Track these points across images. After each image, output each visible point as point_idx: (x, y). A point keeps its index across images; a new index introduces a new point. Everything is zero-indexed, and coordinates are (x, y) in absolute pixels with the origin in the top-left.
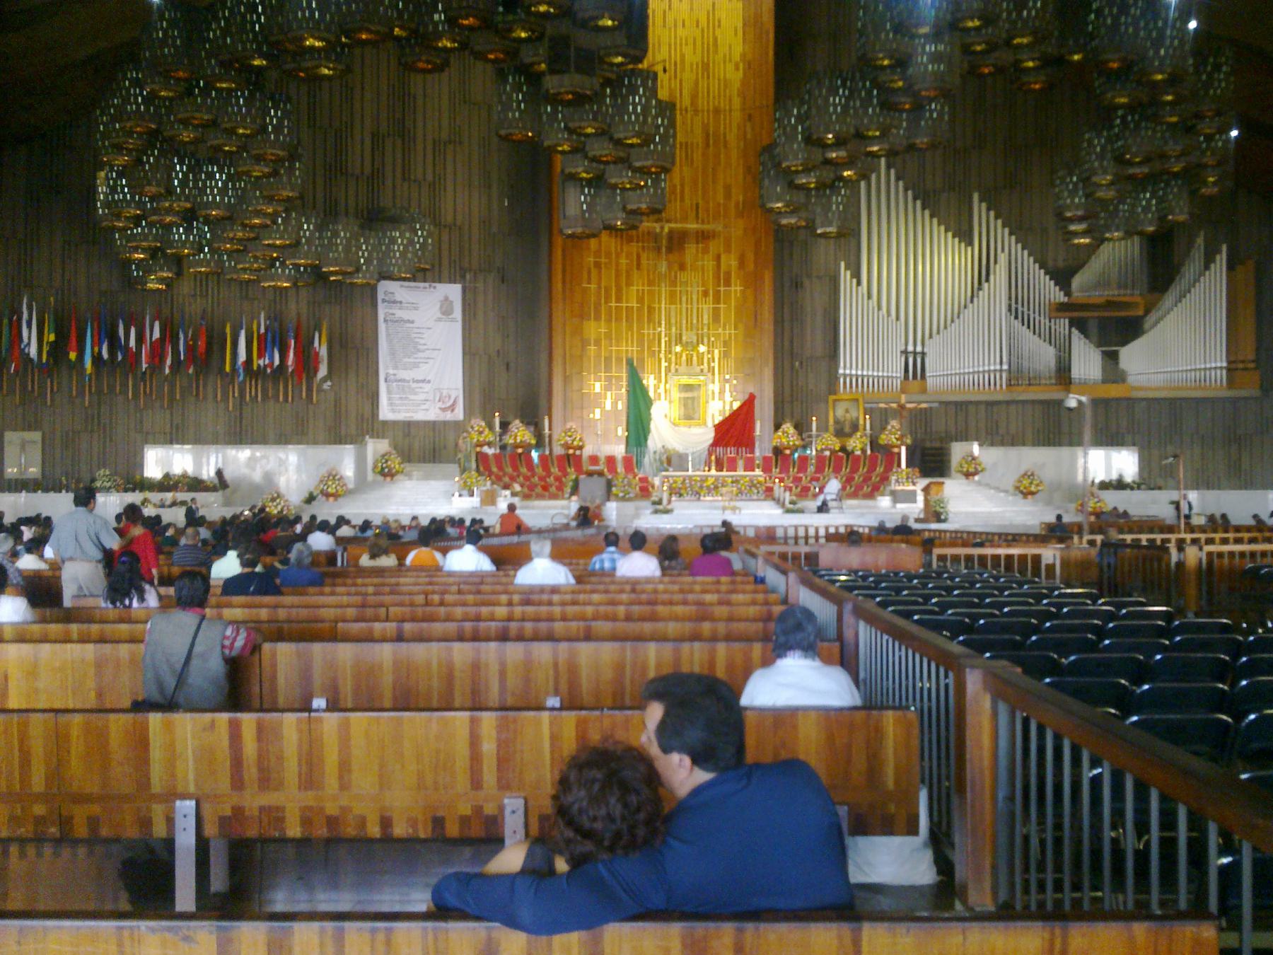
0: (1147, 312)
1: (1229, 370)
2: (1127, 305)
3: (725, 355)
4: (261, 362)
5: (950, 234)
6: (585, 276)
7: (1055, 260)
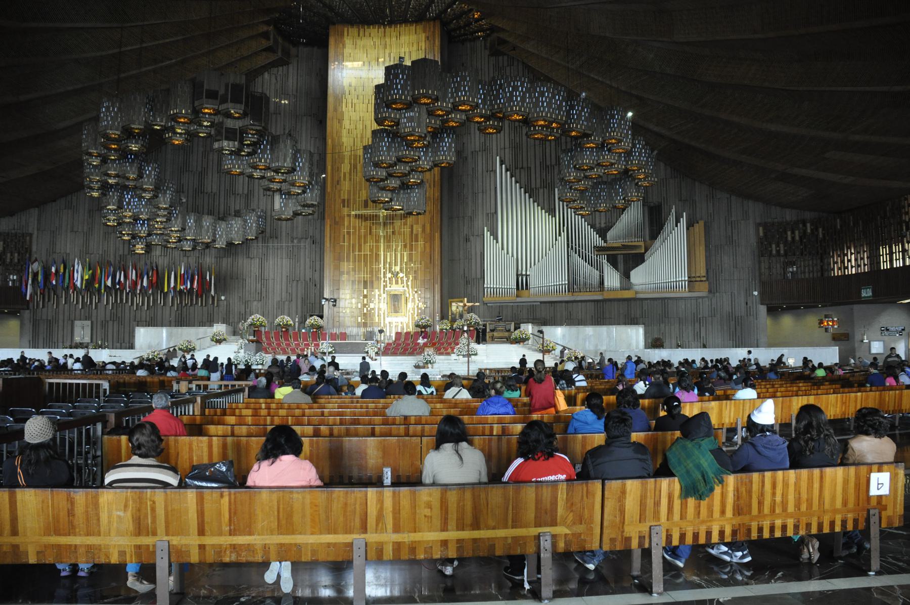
0: (646, 250)
1: (689, 282)
3: (415, 278)
4: (182, 288)
5: (543, 211)
6: (342, 239)
7: (600, 223)
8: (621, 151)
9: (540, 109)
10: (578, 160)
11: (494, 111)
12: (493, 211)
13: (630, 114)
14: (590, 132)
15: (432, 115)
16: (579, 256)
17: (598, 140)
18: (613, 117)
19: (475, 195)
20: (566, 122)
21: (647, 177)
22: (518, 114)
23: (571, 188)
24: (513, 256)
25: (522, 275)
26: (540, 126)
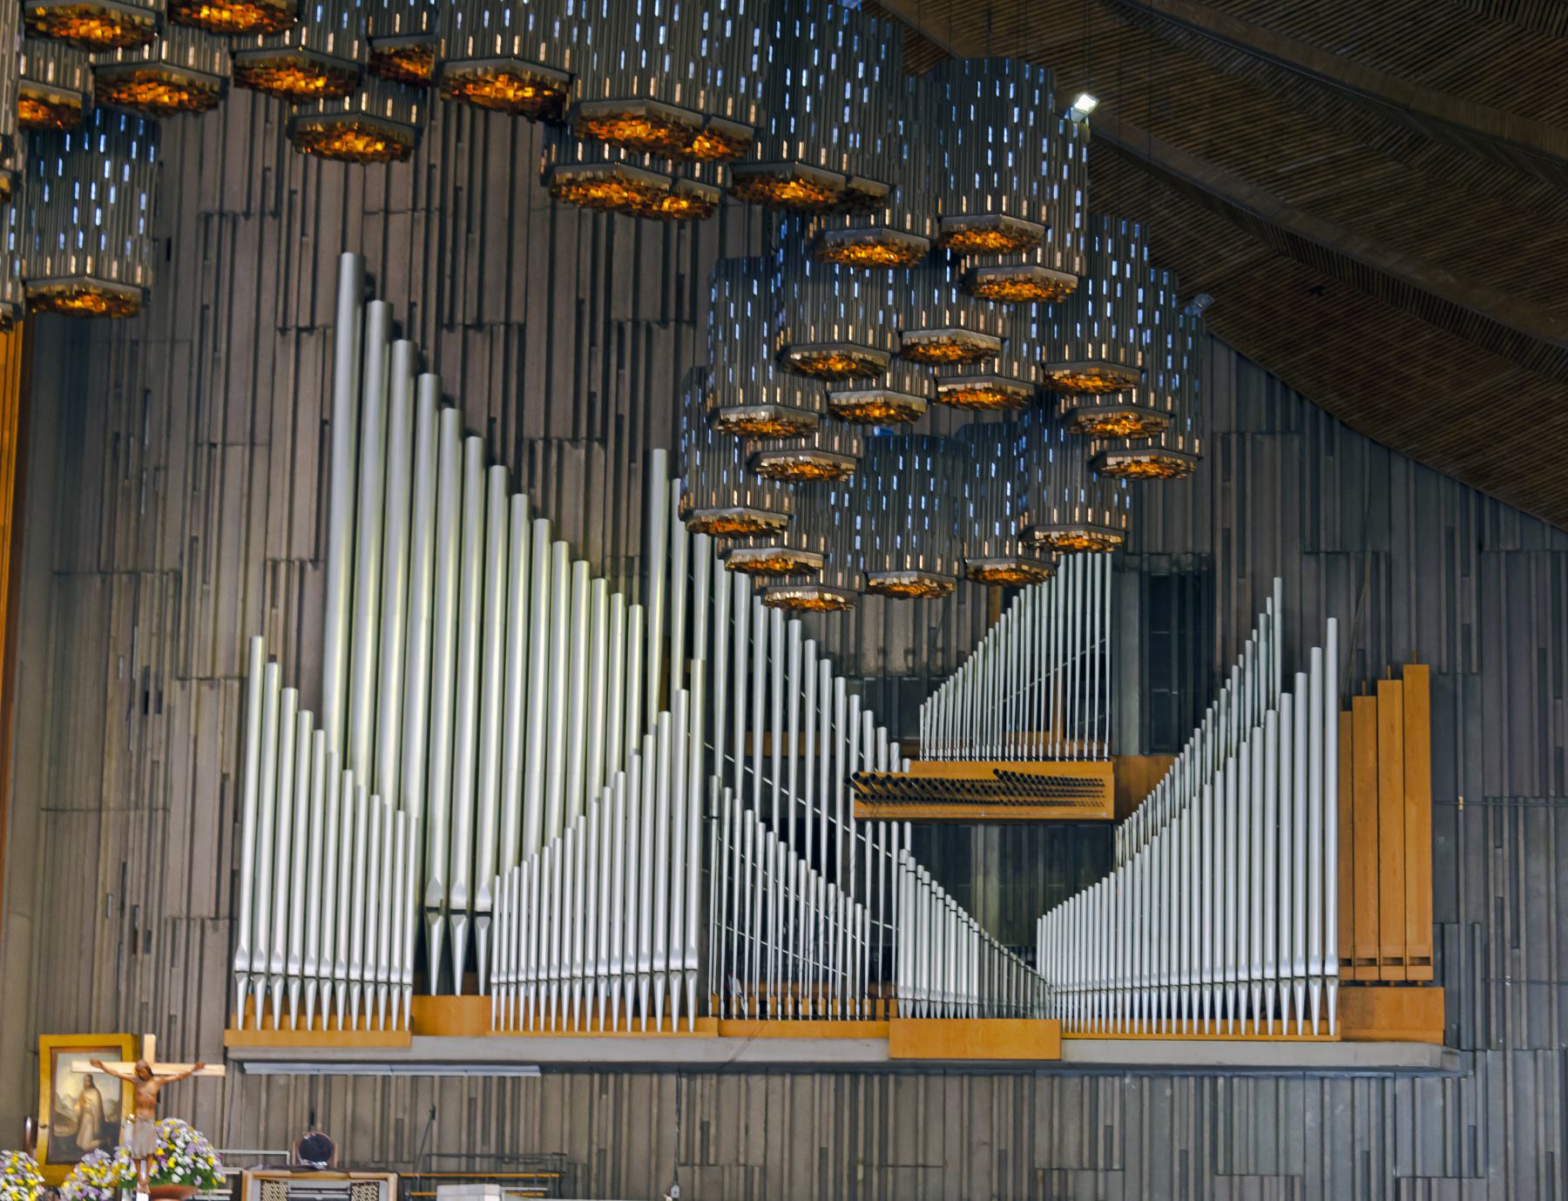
0: (1124, 808)
1: (1344, 985)
2: (1067, 788)
5: (583, 567)
7: (884, 652)
8: (1027, 291)
9: (633, 59)
10: (800, 328)
11: (387, 47)
12: (303, 548)
13: (1085, 103)
14: (876, 189)
15: (47, 35)
16: (767, 820)
17: (917, 231)
18: (996, 112)
19: (206, 451)
20: (759, 132)
21: (1151, 430)
22: (514, 77)
23: (751, 464)
24: (400, 803)
25: (448, 912)
26: (627, 144)
